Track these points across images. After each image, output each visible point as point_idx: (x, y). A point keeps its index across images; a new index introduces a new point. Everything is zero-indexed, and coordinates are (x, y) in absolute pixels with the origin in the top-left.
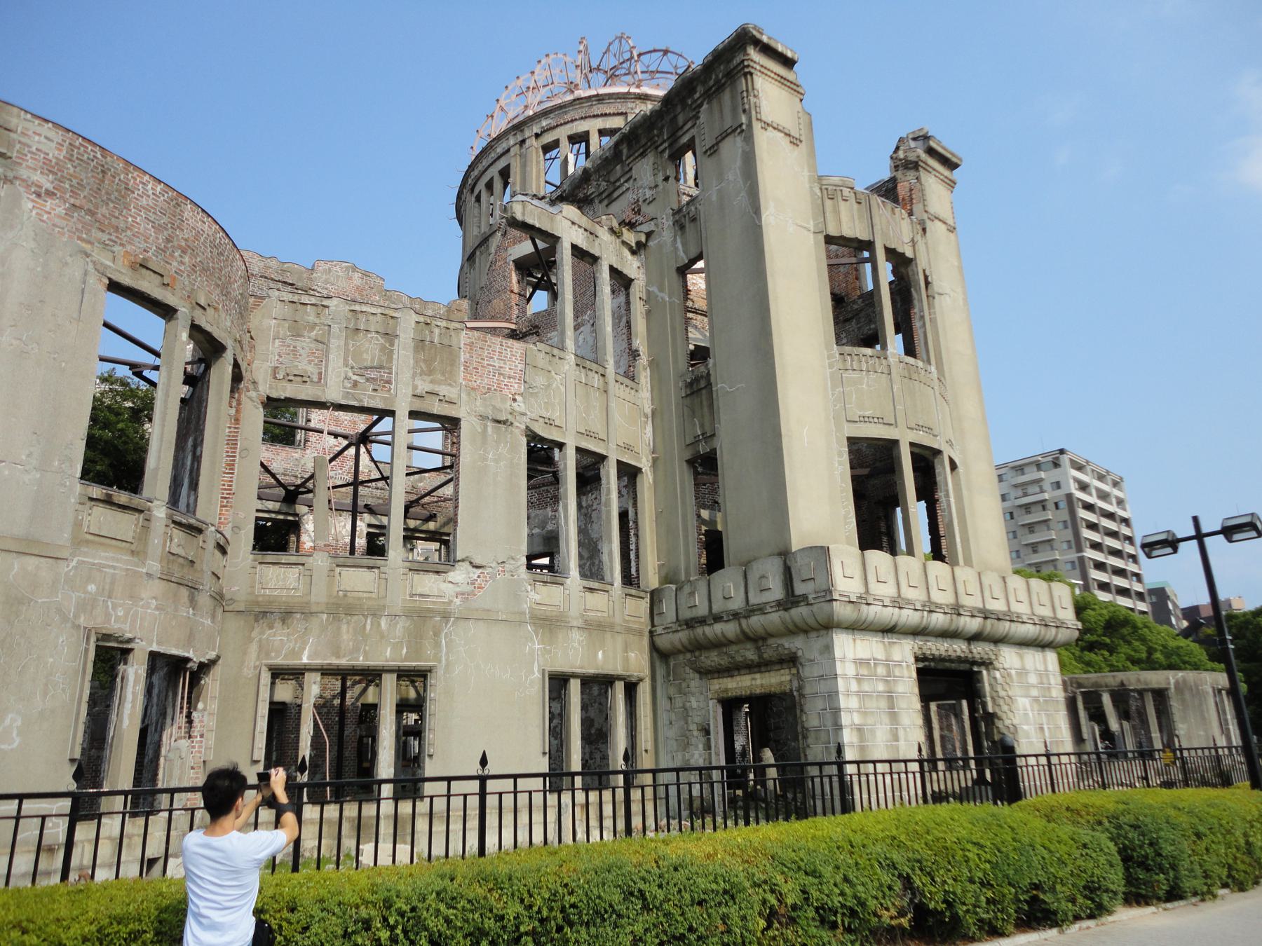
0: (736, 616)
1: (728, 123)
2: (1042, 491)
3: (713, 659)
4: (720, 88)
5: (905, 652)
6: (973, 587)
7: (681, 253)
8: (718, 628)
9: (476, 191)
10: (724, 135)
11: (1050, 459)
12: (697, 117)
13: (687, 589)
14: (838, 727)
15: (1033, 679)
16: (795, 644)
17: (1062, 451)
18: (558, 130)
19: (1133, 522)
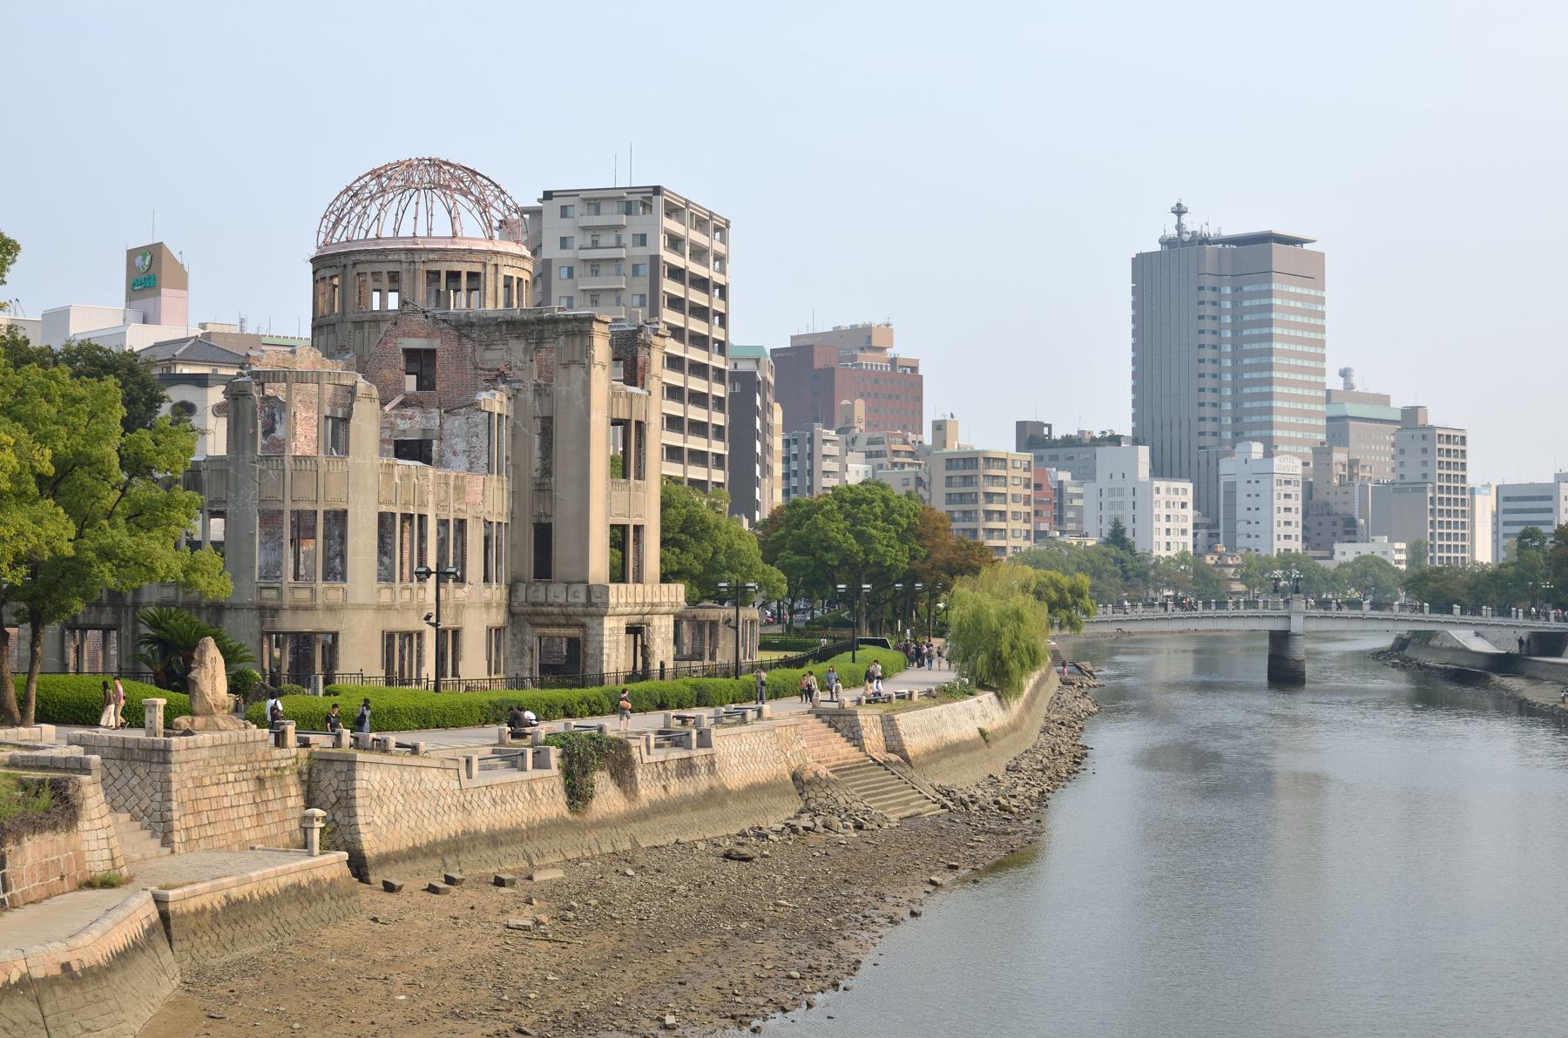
0: (560, 605)
1: (577, 358)
2: (619, 246)
3: (542, 620)
4: (573, 334)
5: (623, 625)
6: (650, 595)
7: (538, 409)
8: (550, 609)
9: (360, 268)
10: (574, 362)
11: (638, 197)
12: (556, 339)
13: (533, 588)
14: (602, 654)
15: (663, 630)
16: (587, 620)
17: (657, 190)
18: (439, 264)
19: (732, 293)
